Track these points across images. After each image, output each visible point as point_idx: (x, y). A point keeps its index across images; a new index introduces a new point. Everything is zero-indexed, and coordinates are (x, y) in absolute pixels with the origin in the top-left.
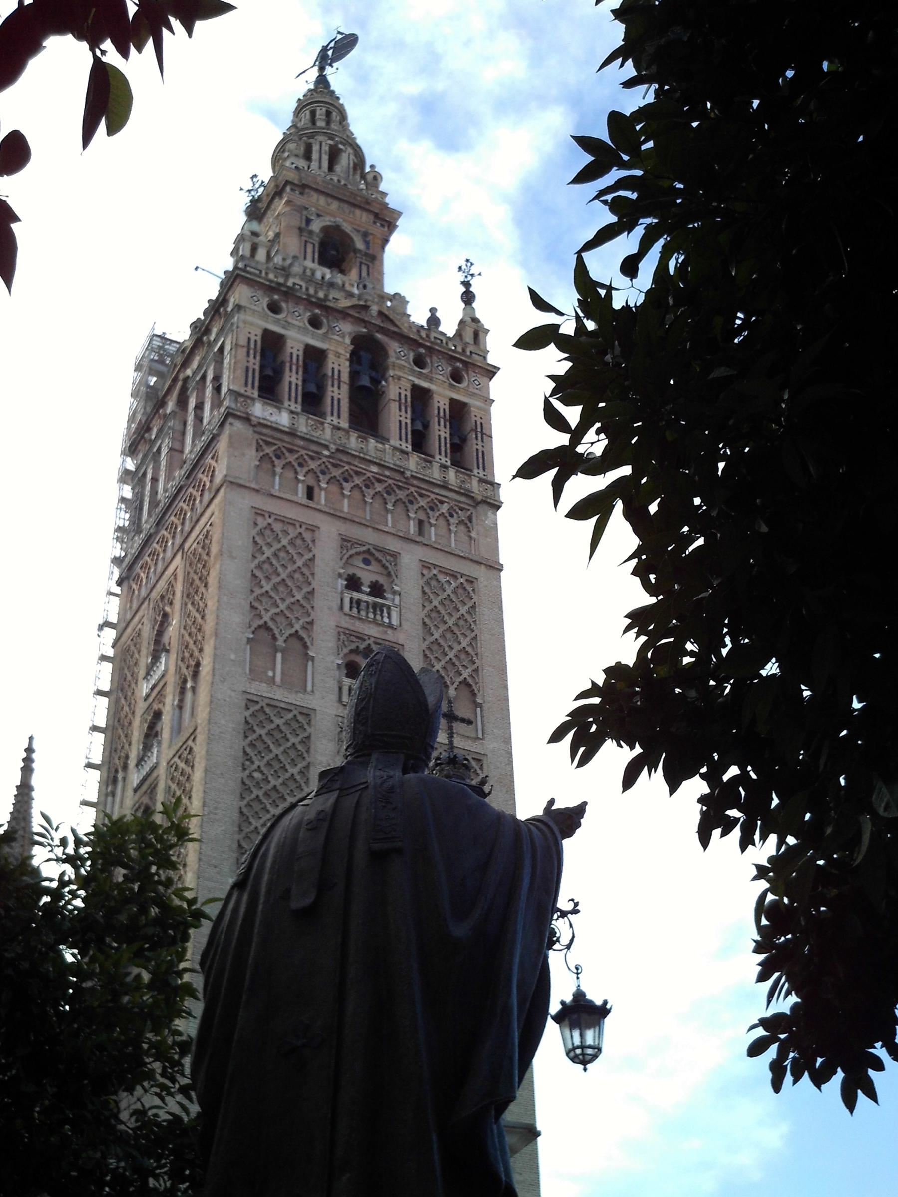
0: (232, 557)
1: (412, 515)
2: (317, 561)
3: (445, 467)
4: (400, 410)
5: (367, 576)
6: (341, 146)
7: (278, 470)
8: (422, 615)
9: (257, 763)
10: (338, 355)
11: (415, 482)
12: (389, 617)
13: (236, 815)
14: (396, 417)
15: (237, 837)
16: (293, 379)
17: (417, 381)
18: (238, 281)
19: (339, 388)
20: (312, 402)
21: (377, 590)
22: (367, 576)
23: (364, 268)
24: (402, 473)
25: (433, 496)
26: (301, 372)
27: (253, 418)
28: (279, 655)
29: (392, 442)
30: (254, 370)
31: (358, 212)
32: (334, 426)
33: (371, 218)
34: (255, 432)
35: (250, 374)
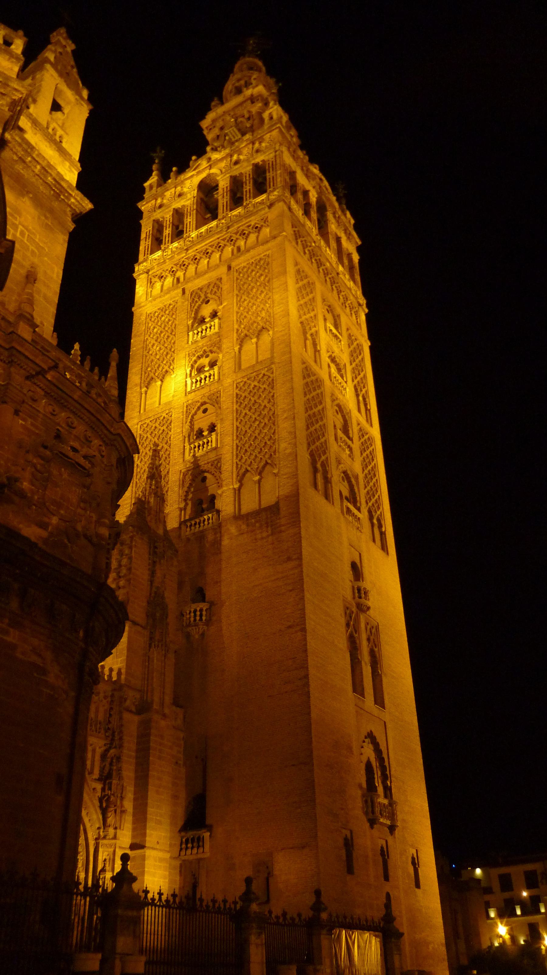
7: (299, 241)
18: (277, 130)
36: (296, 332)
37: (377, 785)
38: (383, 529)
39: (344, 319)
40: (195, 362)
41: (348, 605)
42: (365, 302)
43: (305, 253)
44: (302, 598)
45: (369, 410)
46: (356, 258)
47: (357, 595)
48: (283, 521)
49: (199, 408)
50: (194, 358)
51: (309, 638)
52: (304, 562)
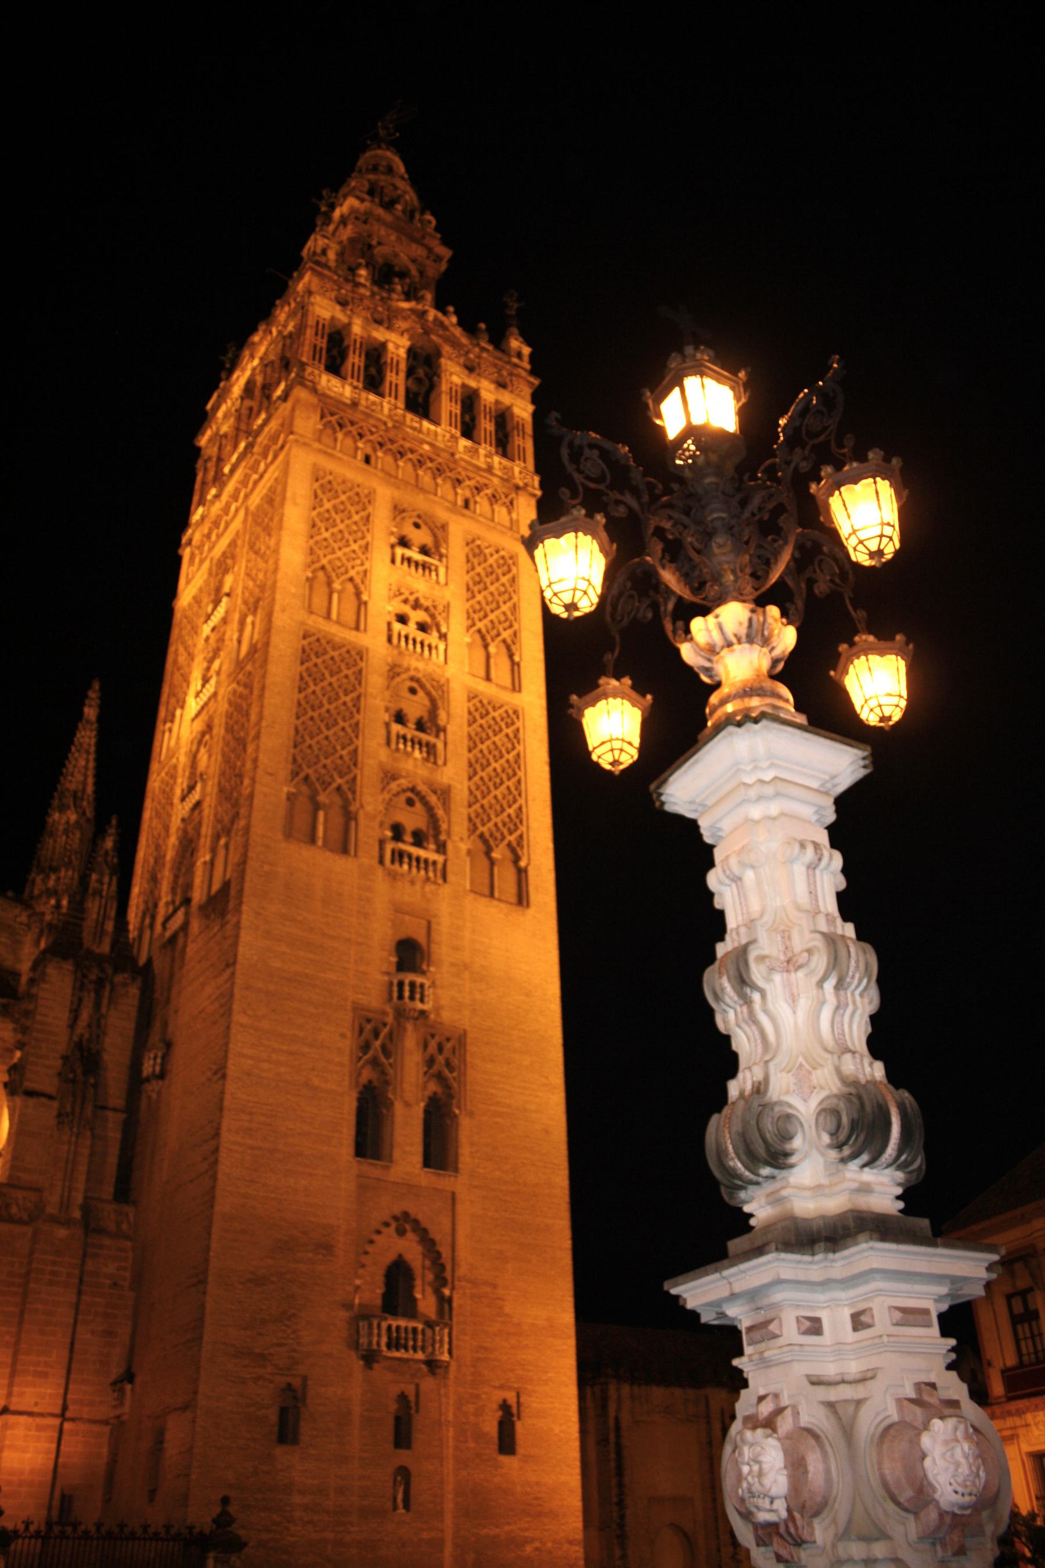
0: (295, 504)
1: (459, 491)
4: (451, 401)
8: (467, 578)
9: (312, 688)
10: (397, 347)
12: (437, 575)
13: (292, 732)
14: (448, 407)
15: (292, 750)
16: (357, 360)
19: (397, 374)
24: (453, 455)
25: (478, 478)
26: (363, 356)
27: (319, 387)
28: (335, 596)
29: (443, 426)
30: (321, 349)
31: (414, 246)
32: (388, 407)
34: (320, 400)
36: (293, 590)
37: (419, 1296)
38: (523, 864)
39: (459, 529)
40: (208, 669)
41: (371, 1015)
42: (537, 479)
43: (357, 448)
44: (228, 1028)
45: (518, 664)
46: (523, 410)
47: (395, 994)
48: (231, 905)
49: (200, 743)
50: (205, 665)
51: (230, 1087)
52: (238, 966)
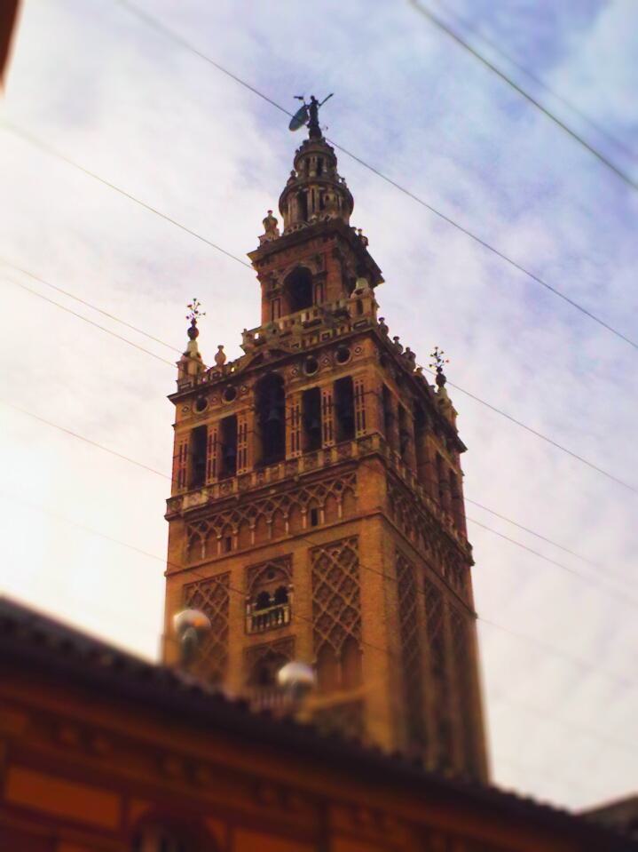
2: (231, 602)
3: (328, 450)
5: (271, 588)
6: (305, 190)
11: (305, 480)
12: (283, 619)
16: (212, 457)
17: (304, 388)
20: (229, 465)
21: (282, 596)
22: (271, 588)
23: (319, 287)
24: (292, 481)
31: (310, 244)
33: (321, 239)
35: (182, 474)
